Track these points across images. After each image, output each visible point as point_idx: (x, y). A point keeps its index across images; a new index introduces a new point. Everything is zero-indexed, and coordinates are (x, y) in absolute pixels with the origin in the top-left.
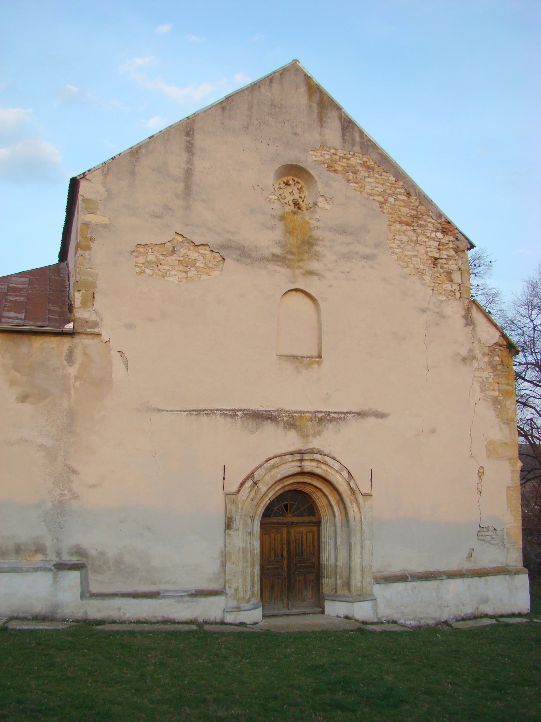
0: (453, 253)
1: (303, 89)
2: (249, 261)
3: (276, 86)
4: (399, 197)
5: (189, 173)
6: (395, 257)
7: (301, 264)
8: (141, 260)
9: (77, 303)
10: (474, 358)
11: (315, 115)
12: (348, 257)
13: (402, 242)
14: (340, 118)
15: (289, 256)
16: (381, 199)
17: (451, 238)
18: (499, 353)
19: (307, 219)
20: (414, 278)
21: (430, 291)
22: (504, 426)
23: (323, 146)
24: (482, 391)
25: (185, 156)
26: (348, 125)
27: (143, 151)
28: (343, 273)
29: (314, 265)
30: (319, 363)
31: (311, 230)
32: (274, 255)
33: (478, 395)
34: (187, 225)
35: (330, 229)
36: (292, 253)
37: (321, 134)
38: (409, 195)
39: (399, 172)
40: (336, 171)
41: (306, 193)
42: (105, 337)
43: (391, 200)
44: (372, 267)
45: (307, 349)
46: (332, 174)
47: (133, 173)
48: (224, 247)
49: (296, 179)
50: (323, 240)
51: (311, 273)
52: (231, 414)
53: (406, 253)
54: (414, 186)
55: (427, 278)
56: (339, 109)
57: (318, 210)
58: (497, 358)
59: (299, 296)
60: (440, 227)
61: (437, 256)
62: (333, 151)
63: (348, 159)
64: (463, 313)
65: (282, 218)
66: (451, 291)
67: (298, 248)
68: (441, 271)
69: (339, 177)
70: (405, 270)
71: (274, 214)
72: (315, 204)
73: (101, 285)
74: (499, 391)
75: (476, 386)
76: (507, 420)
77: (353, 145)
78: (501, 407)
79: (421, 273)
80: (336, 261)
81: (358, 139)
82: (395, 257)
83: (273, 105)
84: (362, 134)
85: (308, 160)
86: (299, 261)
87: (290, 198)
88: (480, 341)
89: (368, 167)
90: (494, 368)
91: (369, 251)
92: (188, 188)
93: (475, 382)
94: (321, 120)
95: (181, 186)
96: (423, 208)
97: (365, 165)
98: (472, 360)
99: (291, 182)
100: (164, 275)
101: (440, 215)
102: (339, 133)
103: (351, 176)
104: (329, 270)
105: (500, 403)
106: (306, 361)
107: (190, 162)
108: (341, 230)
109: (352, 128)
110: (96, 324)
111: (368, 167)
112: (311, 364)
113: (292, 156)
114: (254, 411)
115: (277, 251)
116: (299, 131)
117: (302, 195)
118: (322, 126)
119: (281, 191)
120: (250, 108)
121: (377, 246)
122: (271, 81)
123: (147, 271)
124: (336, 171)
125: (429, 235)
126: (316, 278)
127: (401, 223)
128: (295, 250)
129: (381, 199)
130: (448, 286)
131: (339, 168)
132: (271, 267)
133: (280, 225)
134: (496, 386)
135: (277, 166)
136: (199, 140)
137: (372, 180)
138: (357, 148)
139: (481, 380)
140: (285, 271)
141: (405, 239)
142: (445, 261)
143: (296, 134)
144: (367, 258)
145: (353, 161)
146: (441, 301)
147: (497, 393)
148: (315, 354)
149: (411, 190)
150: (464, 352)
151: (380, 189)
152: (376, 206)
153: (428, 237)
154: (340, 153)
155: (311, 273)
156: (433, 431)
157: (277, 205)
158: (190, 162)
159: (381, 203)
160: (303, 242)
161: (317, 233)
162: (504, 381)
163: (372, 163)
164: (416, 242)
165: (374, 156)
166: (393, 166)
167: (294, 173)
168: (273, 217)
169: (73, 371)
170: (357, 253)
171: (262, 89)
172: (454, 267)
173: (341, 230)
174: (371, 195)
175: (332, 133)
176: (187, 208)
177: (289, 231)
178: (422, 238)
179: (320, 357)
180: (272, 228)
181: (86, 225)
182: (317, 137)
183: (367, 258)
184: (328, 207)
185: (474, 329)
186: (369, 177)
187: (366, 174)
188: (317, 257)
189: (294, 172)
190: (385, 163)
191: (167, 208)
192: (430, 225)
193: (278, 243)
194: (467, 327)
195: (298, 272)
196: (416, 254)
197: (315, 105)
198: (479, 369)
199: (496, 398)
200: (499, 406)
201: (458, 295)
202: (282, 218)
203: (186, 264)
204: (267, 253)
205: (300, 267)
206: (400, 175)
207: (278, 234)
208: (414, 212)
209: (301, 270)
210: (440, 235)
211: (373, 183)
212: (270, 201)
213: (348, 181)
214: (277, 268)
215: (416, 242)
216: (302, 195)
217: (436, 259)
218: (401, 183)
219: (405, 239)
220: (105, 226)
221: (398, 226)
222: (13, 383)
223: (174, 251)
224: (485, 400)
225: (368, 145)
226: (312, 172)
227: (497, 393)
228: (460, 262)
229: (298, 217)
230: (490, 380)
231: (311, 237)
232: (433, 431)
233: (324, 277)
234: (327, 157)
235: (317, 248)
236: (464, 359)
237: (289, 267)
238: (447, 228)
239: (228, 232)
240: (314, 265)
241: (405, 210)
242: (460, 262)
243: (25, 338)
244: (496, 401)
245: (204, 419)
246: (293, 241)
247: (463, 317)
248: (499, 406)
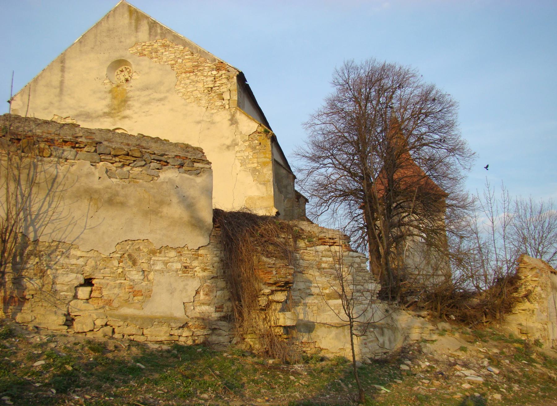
0: (225, 81)
1: (126, 15)
2: (90, 119)
3: (111, 19)
4: (186, 57)
5: (62, 82)
6: (181, 95)
7: (119, 114)
10: (237, 145)
11: (133, 28)
12: (147, 103)
13: (185, 84)
14: (148, 23)
15: (113, 111)
17: (224, 72)
18: (258, 138)
19: (125, 88)
20: (193, 104)
21: (204, 109)
22: (260, 186)
25: (60, 74)
26: (153, 25)
27: (40, 78)
28: (144, 112)
29: (127, 112)
31: (127, 93)
33: (239, 167)
34: (60, 109)
35: (138, 90)
36: (115, 109)
37: (136, 37)
38: (192, 54)
39: (186, 42)
40: (145, 55)
44: (163, 105)
49: (126, 67)
50: (133, 97)
51: (125, 117)
53: (188, 90)
56: (147, 18)
58: (256, 142)
60: (215, 67)
61: (212, 86)
62: (143, 44)
63: (153, 45)
64: (230, 117)
66: (221, 105)
67: (119, 105)
68: (214, 94)
69: (146, 58)
70: (187, 100)
71: (106, 90)
74: (258, 163)
75: (238, 163)
76: (264, 181)
77: (156, 36)
78: (259, 173)
79: (198, 100)
80: (140, 107)
81: (159, 31)
82: (181, 95)
83: (109, 30)
85: (127, 54)
86: (118, 113)
88: (241, 133)
90: (254, 148)
91: (162, 96)
92: (61, 90)
93: (237, 161)
94: (137, 29)
95: (58, 90)
96: (202, 59)
97: (164, 46)
98: (234, 146)
99: (124, 70)
102: (148, 32)
103: (154, 55)
104: (136, 113)
105: (258, 171)
107: (63, 76)
108: (146, 88)
109: (156, 26)
115: (107, 110)
116: (123, 39)
117: (130, 75)
119: (118, 76)
120: (96, 36)
121: (168, 91)
122: (108, 17)
124: (145, 55)
125: (206, 74)
126: (127, 119)
127: (185, 73)
128: (116, 107)
129: (173, 62)
130: (219, 103)
131: (146, 53)
133: (109, 96)
134: (255, 160)
136: (68, 64)
137: (167, 53)
138: (158, 37)
139: (242, 158)
141: (189, 81)
142: (218, 88)
143: (121, 42)
144: (160, 100)
145: (156, 46)
147: (256, 165)
150: (228, 142)
151: (173, 56)
152: (169, 67)
153: (205, 76)
154: (148, 44)
160: (122, 101)
162: (262, 155)
163: (168, 42)
164: (197, 82)
166: (182, 40)
168: (106, 92)
170: (154, 99)
171: (103, 24)
172: (225, 90)
174: (165, 62)
175: (143, 33)
176: (61, 101)
177: (114, 98)
180: (104, 99)
183: (160, 100)
184: (137, 77)
185: (237, 127)
186: (165, 51)
187: (163, 51)
188: (129, 107)
191: (51, 103)
192: (206, 68)
193: (108, 106)
194: (232, 126)
195: (117, 119)
196: (195, 89)
197: (133, 21)
199: (255, 168)
200: (257, 173)
201: (227, 107)
202: (110, 92)
204: (101, 113)
205: (118, 116)
208: (196, 64)
209: (119, 117)
210: (214, 72)
212: (105, 84)
213: (152, 58)
214: (105, 119)
216: (130, 75)
217: (212, 88)
218: (187, 48)
219: (189, 81)
221: (184, 75)
224: (245, 171)
226: (129, 60)
227: (256, 165)
228: (229, 85)
229: (120, 88)
230: (250, 157)
231: (127, 97)
233: (132, 118)
234: (139, 48)
235: (129, 103)
236: (228, 147)
237: (112, 117)
239: (81, 107)
242: (229, 85)
244: (254, 171)
246: (116, 102)
247: (229, 120)
248: (257, 173)
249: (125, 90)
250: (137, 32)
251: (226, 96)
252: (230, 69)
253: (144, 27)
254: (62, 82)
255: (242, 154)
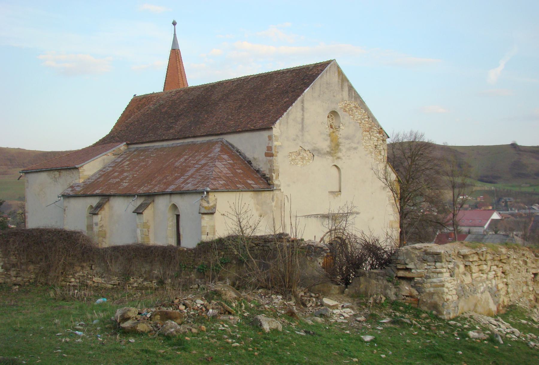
0: (382, 142)
1: (336, 74)
8: (290, 159)
9: (274, 178)
12: (349, 149)
16: (360, 121)
23: (343, 100)
24: (389, 201)
25: (301, 112)
26: (351, 88)
29: (340, 154)
30: (340, 194)
31: (338, 139)
32: (327, 152)
33: (388, 202)
34: (303, 142)
36: (332, 150)
40: (346, 111)
41: (334, 121)
42: (282, 190)
43: (363, 121)
45: (336, 189)
46: (345, 113)
47: (287, 123)
48: (314, 150)
51: (339, 158)
52: (316, 216)
54: (371, 114)
55: (373, 154)
56: (348, 81)
57: (341, 130)
59: (335, 168)
65: (330, 135)
69: (347, 114)
72: (339, 127)
73: (280, 170)
75: (387, 198)
79: (371, 152)
84: (355, 91)
85: (338, 107)
86: (335, 153)
87: (329, 124)
89: (357, 108)
94: (342, 88)
95: (301, 125)
100: (297, 164)
101: (379, 126)
106: (337, 193)
107: (303, 115)
108: (347, 138)
110: (279, 186)
111: (357, 108)
112: (338, 195)
113: (333, 107)
114: (323, 214)
115: (328, 150)
116: (335, 94)
118: (342, 91)
121: (358, 143)
123: (292, 163)
124: (346, 111)
129: (360, 121)
130: (379, 157)
132: (328, 157)
133: (329, 138)
135: (328, 113)
138: (353, 99)
140: (331, 158)
141: (367, 138)
143: (334, 96)
144: (355, 149)
146: (377, 164)
148: (338, 190)
149: (370, 116)
155: (339, 158)
156: (373, 218)
157: (328, 130)
158: (303, 115)
159: (360, 123)
161: (340, 140)
164: (370, 139)
165: (359, 102)
167: (334, 113)
169: (274, 204)
173: (347, 138)
174: (357, 120)
176: (303, 135)
177: (332, 141)
178: (372, 137)
179: (340, 191)
180: (327, 140)
181: (275, 146)
182: (341, 96)
183: (355, 149)
188: (340, 151)
189: (334, 113)
190: (362, 104)
191: (297, 136)
195: (335, 158)
198: (388, 192)
202: (330, 135)
203: (303, 158)
204: (325, 151)
206: (367, 110)
207: (328, 143)
210: (378, 135)
211: (359, 114)
214: (328, 157)
215: (370, 139)
219: (367, 138)
220: (280, 146)
221: (365, 133)
222: (257, 210)
223: (299, 154)
225: (357, 97)
226: (339, 113)
229: (334, 134)
232: (373, 218)
235: (340, 147)
237: (332, 156)
238: (381, 131)
240: (340, 154)
241: (367, 125)
243: (260, 193)
245: (309, 219)
249: (337, 136)
250: (342, 91)
251: (383, 153)
252: (384, 134)
253: (346, 89)
254: (303, 119)
255: (388, 194)
